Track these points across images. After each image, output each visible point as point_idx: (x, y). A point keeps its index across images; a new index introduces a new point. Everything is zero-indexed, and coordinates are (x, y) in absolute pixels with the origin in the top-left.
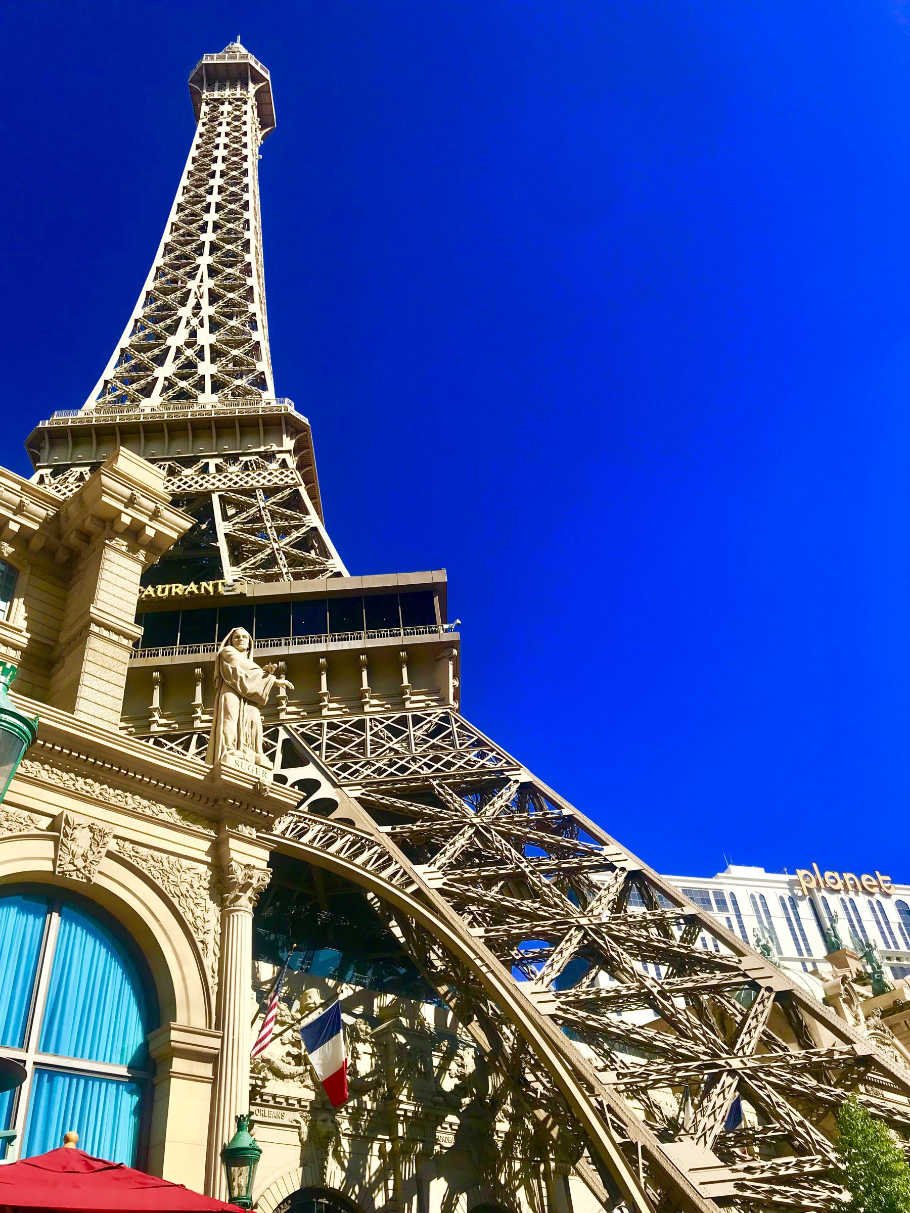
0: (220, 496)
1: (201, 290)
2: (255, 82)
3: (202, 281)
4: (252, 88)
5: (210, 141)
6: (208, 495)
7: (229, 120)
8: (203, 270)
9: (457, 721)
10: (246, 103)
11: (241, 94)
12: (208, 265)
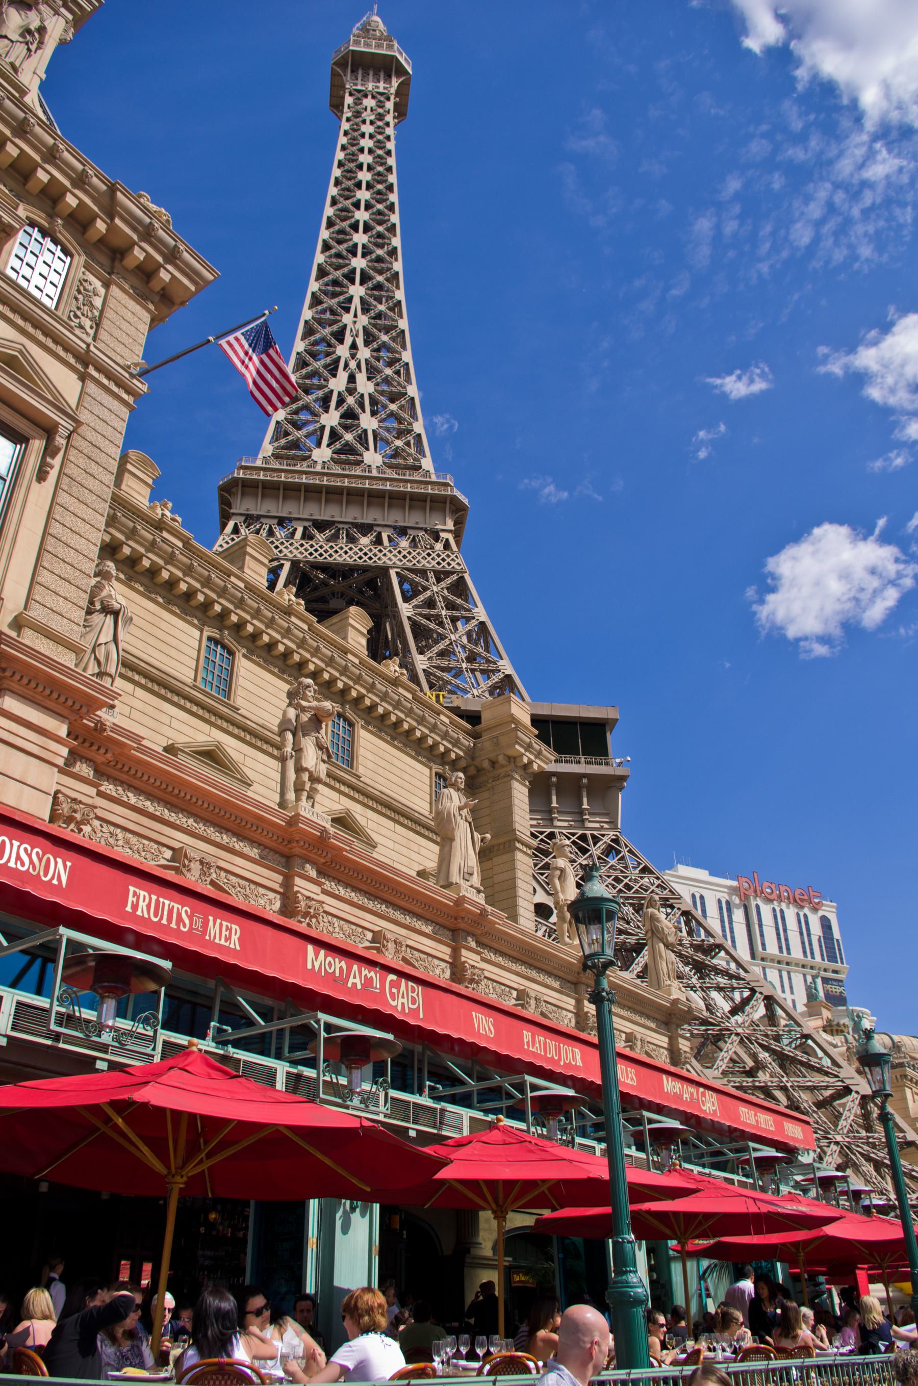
0: (397, 573)
1: (357, 326)
2: (398, 75)
3: (355, 316)
4: (395, 83)
5: (353, 142)
6: (385, 570)
7: (373, 117)
8: (356, 302)
9: (626, 846)
10: (388, 99)
11: (385, 88)
12: (361, 298)
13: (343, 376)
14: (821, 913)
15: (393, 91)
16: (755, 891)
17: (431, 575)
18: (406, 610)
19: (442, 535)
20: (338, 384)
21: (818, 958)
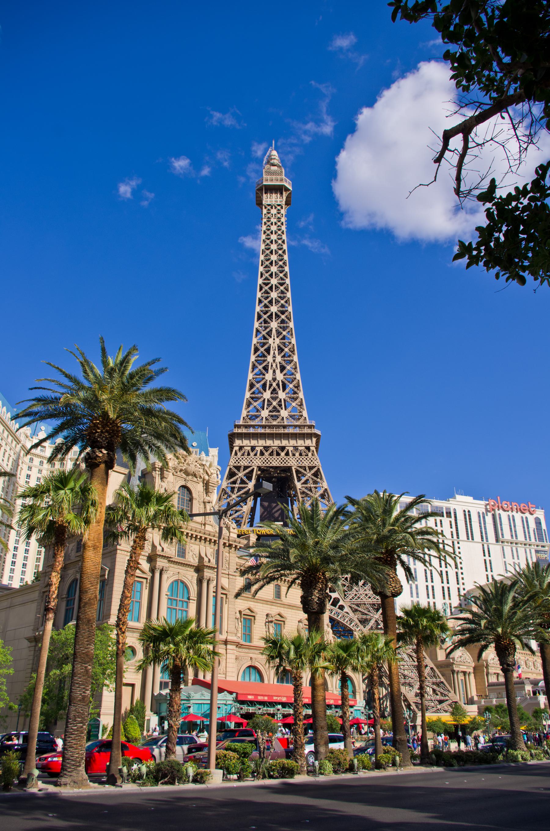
8: (274, 332)
13: (271, 371)
14: (535, 516)
15: (284, 203)
16: (498, 507)
17: (307, 468)
18: (298, 485)
19: (311, 448)
20: (269, 376)
21: (533, 540)
